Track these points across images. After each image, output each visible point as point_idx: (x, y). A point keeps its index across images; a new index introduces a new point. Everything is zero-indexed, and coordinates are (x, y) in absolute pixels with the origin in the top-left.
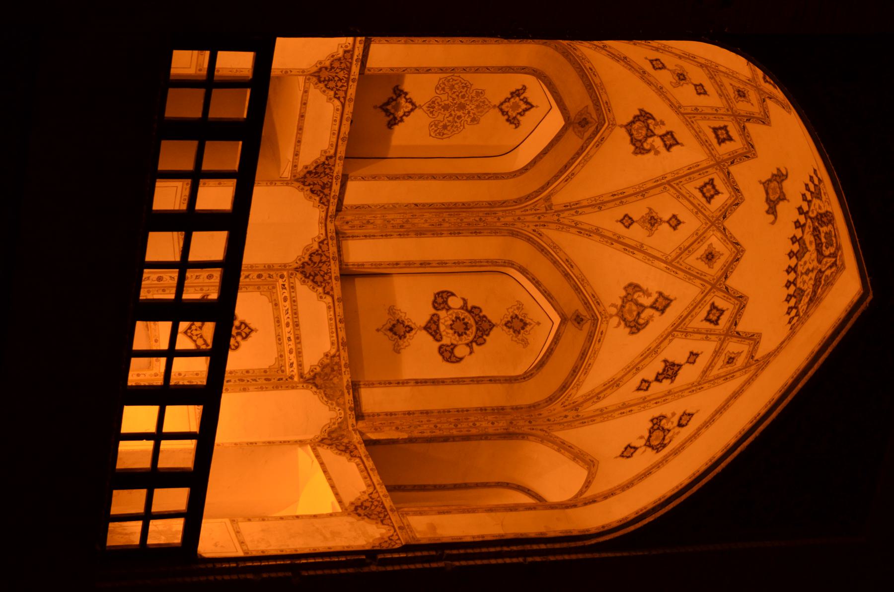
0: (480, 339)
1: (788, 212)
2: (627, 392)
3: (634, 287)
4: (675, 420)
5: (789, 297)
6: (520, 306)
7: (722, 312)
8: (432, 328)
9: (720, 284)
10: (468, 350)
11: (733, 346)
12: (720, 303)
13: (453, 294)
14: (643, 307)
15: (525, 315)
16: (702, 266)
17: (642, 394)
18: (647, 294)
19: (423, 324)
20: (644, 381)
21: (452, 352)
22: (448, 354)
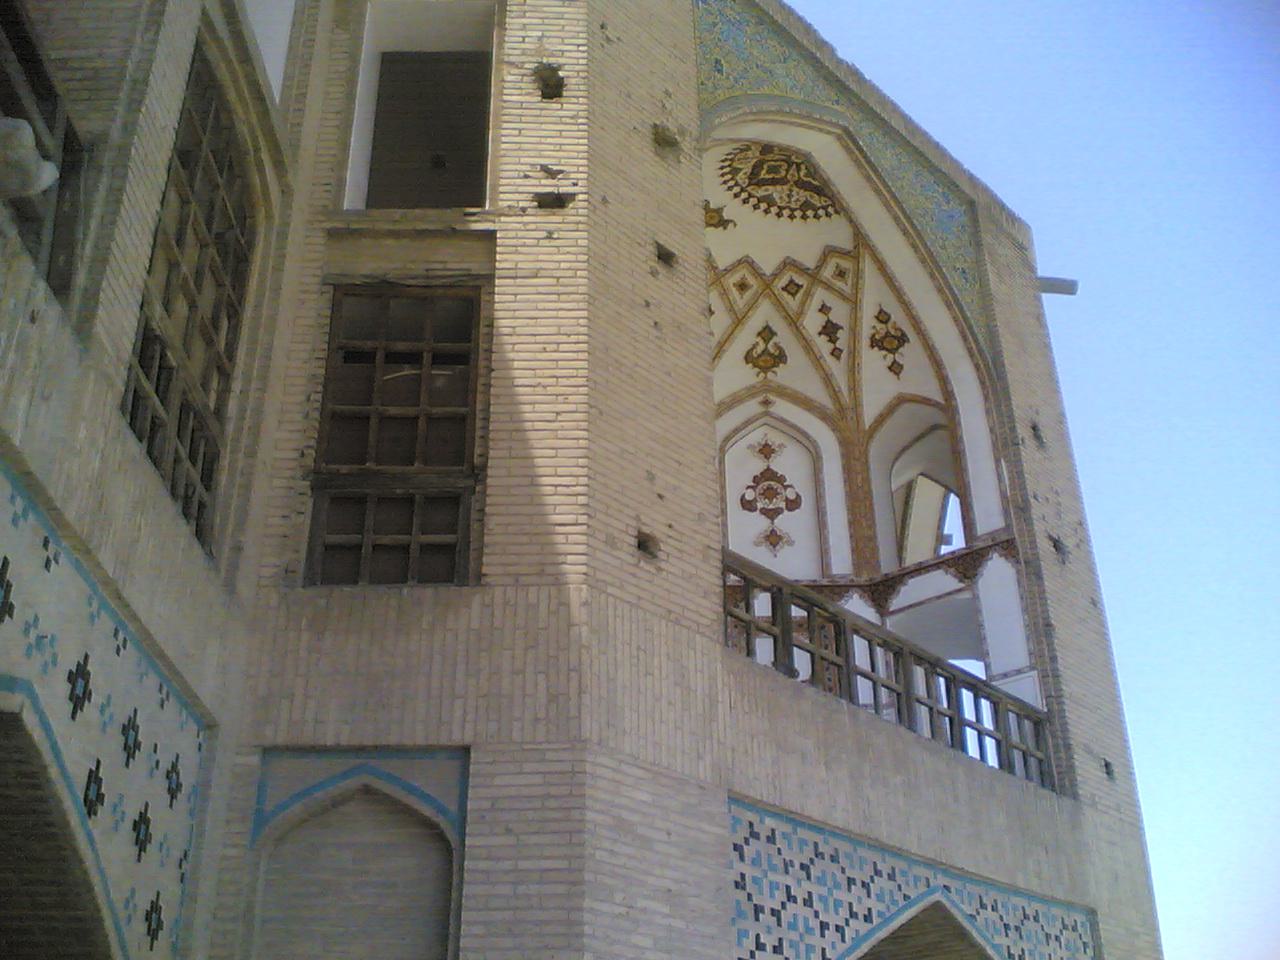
0: (781, 479)
1: (733, 209)
2: (838, 369)
3: (748, 358)
4: (879, 326)
5: (804, 217)
6: (751, 447)
7: (791, 281)
8: (771, 514)
9: (767, 283)
10: (789, 489)
11: (828, 272)
12: (783, 281)
13: (743, 497)
14: (765, 351)
15: (759, 444)
16: (748, 294)
17: (844, 355)
18: (754, 346)
19: (769, 521)
20: (832, 354)
21: (792, 501)
22: (793, 504)
